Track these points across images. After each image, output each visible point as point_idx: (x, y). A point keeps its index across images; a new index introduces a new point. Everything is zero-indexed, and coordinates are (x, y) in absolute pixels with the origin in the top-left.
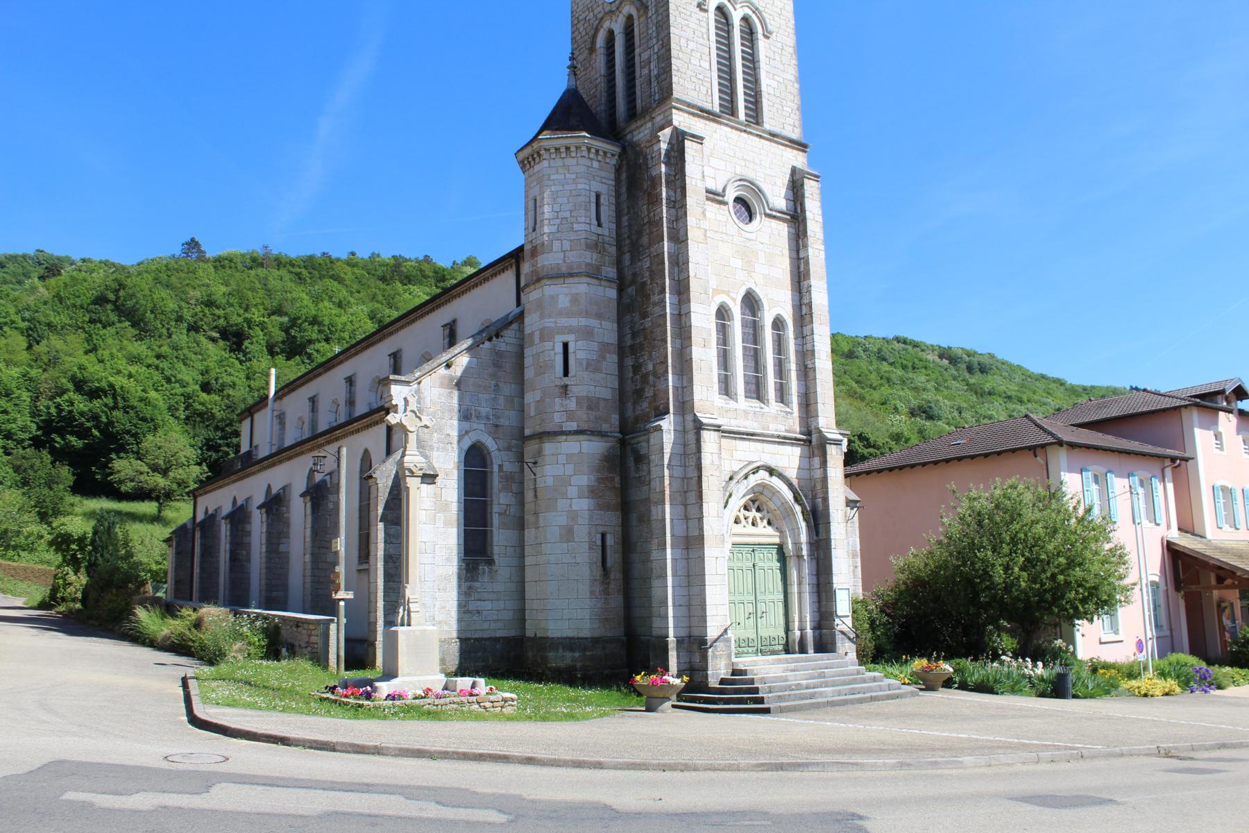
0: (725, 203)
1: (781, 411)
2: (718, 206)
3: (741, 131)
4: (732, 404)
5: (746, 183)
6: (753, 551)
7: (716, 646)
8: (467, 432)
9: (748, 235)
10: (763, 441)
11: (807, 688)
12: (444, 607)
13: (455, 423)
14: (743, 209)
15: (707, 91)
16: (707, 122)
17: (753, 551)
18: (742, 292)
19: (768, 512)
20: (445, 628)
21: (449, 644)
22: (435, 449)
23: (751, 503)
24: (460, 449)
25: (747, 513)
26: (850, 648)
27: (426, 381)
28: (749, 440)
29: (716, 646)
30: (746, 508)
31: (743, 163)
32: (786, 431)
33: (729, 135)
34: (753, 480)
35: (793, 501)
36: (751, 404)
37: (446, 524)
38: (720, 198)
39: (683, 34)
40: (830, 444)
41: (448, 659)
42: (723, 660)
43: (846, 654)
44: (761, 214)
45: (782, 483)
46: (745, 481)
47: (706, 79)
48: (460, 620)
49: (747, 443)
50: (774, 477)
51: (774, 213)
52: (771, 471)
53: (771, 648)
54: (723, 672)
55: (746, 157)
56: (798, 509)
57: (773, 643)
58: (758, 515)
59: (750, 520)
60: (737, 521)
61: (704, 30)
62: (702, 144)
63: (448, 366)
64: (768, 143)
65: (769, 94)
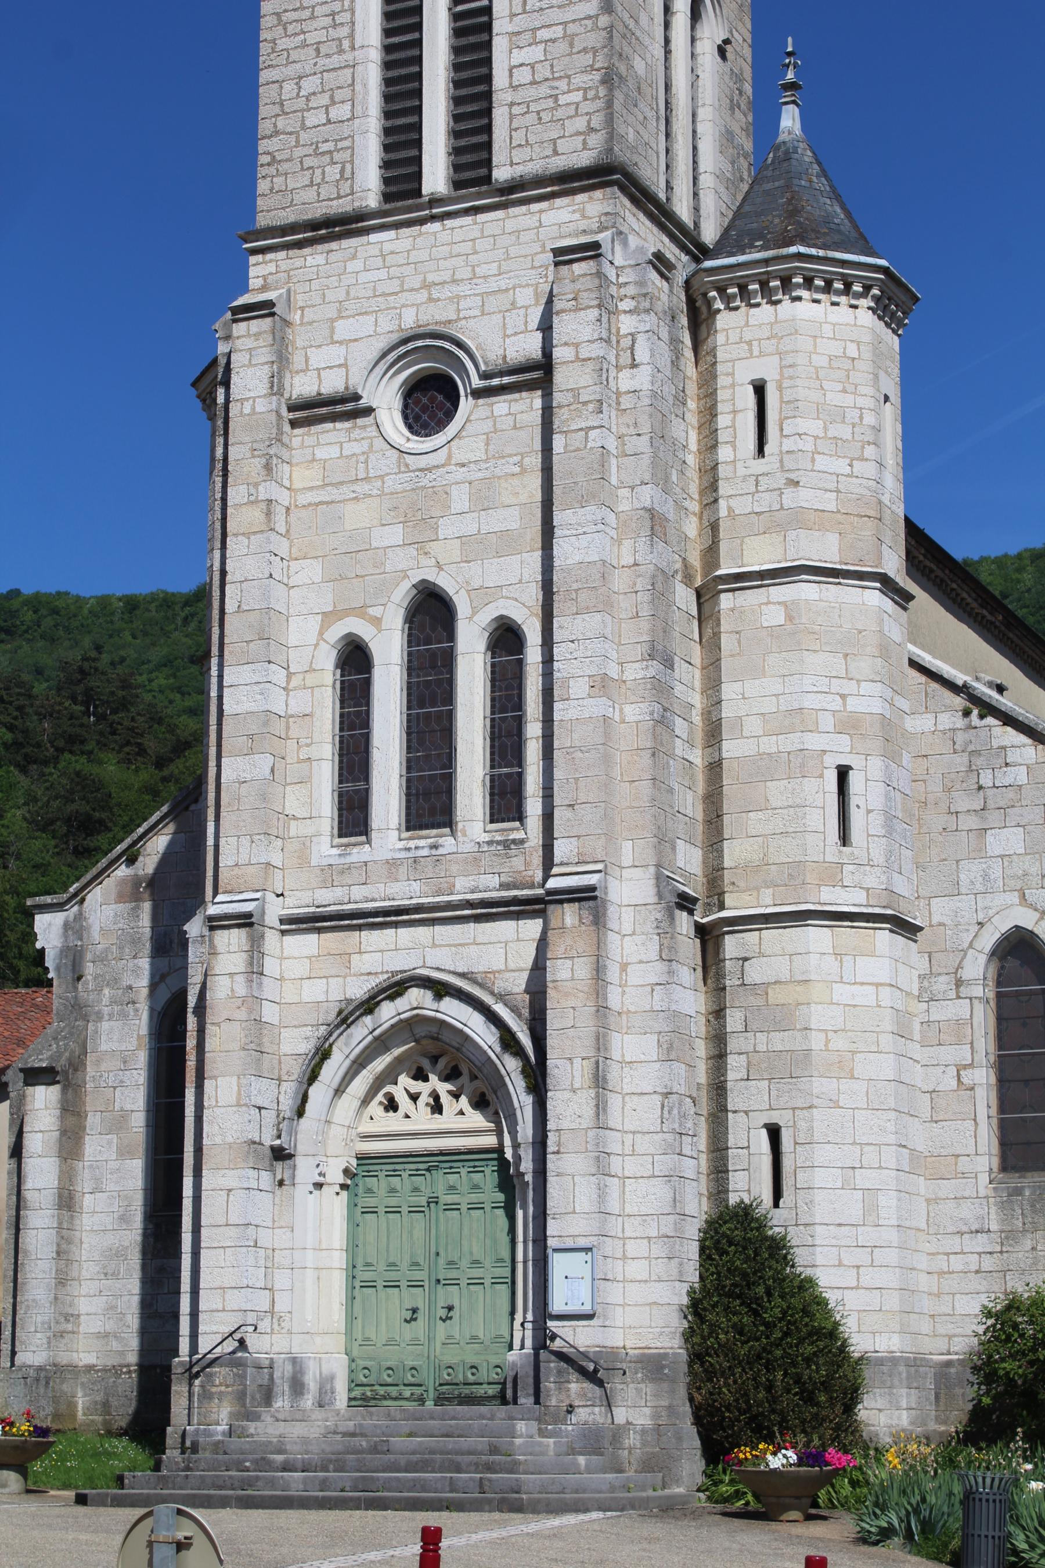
0: (369, 411)
1: (490, 843)
2: (347, 425)
3: (421, 222)
4: (360, 853)
5: (420, 343)
6: (428, 1170)
7: (211, 1375)
8: (163, 977)
9: (423, 461)
10: (433, 922)
11: (285, 1469)
12: (113, 1307)
13: (144, 963)
14: (440, 398)
15: (342, 171)
16: (334, 245)
17: (428, 1170)
18: (401, 595)
19: (474, 1077)
20: (115, 1345)
21: (118, 1375)
22: (106, 1017)
23: (426, 1064)
24: (152, 1010)
25: (416, 1086)
26: (583, 1395)
27: (96, 896)
28: (396, 925)
29: (211, 1375)
30: (420, 1075)
31: (423, 295)
32: (504, 886)
33: (387, 247)
34: (388, 1012)
35: (498, 1049)
36: (412, 844)
37: (124, 1153)
38: (349, 406)
39: (291, 70)
40: (561, 902)
41: (114, 1402)
42: (225, 1403)
43: (570, 1409)
44: (466, 396)
45: (471, 1010)
46: (368, 1020)
47: (340, 145)
48: (144, 1332)
49: (390, 932)
50: (447, 999)
51: (496, 382)
52: (440, 990)
53: (466, 1391)
54: (219, 1428)
55: (430, 278)
56: (511, 1065)
57: (471, 1378)
58: (443, 1088)
59: (424, 1099)
60: (391, 1105)
61: (344, 31)
62: (273, 314)
63: (131, 861)
64: (499, 214)
65: (514, 88)
